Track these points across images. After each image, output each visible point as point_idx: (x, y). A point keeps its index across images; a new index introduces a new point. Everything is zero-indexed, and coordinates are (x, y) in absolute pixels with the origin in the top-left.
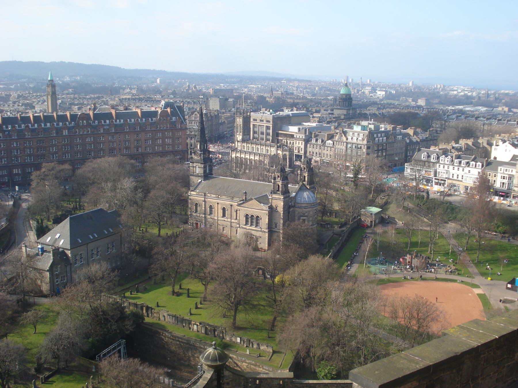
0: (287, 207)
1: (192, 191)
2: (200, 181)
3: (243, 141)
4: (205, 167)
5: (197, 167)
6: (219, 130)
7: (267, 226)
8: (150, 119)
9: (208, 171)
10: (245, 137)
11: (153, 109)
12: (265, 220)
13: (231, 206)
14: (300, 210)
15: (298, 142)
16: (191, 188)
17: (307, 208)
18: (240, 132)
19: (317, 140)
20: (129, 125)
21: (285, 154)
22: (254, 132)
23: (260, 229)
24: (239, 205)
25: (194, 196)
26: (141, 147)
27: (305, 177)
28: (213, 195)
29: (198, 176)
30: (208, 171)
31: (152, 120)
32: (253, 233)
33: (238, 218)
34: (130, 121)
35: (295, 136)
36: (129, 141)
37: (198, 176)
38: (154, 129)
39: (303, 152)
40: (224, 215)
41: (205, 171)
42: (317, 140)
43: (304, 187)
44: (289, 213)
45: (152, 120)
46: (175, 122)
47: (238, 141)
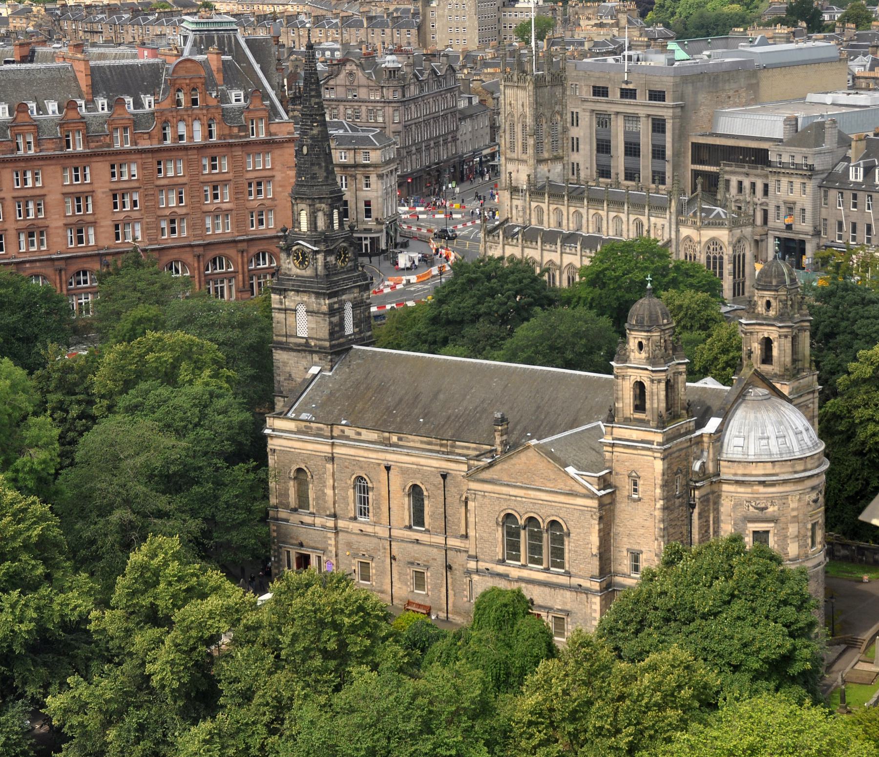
0: (680, 481)
1: (282, 415)
2: (315, 370)
3: (537, 190)
4: (335, 312)
5: (302, 310)
6: (455, 139)
7: (594, 566)
8: (129, 100)
9: (349, 329)
10: (543, 169)
11: (145, 58)
12: (583, 541)
13: (444, 477)
15: (784, 181)
16: (280, 403)
17: (773, 484)
18: (525, 150)
20: (37, 127)
21: (714, 241)
22: (604, 147)
23: (564, 580)
24: (469, 477)
25: (287, 437)
26: (94, 224)
27: (767, 343)
28: (367, 435)
29: (305, 348)
30: (349, 329)
31: (138, 104)
32: (532, 593)
33: (472, 533)
34: (41, 109)
35: (773, 157)
36: (39, 199)
37: (305, 348)
38: (145, 144)
40: (418, 519)
41: (336, 330)
43: (762, 391)
45: (138, 104)
46: (241, 111)
47: (514, 190)
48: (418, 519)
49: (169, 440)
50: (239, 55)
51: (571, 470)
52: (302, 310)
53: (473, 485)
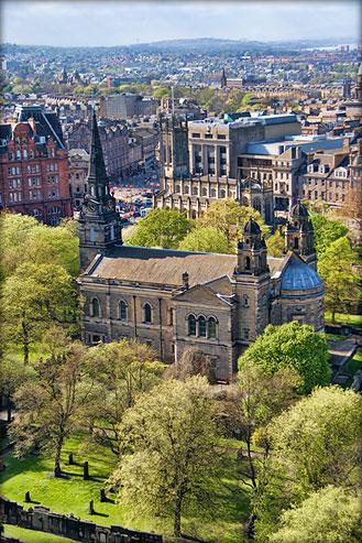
5: (92, 230)
9: (113, 237)
13: (160, 300)
14: (291, 303)
19: (316, 169)
21: (257, 198)
22: (197, 159)
30: (113, 237)
35: (274, 163)
39: (290, 193)
40: (148, 319)
42: (316, 169)
44: (270, 309)
47: (167, 178)
48: (148, 319)
49: (40, 287)
50: (43, 121)
51: (219, 295)
52: (92, 230)
53: (175, 303)
